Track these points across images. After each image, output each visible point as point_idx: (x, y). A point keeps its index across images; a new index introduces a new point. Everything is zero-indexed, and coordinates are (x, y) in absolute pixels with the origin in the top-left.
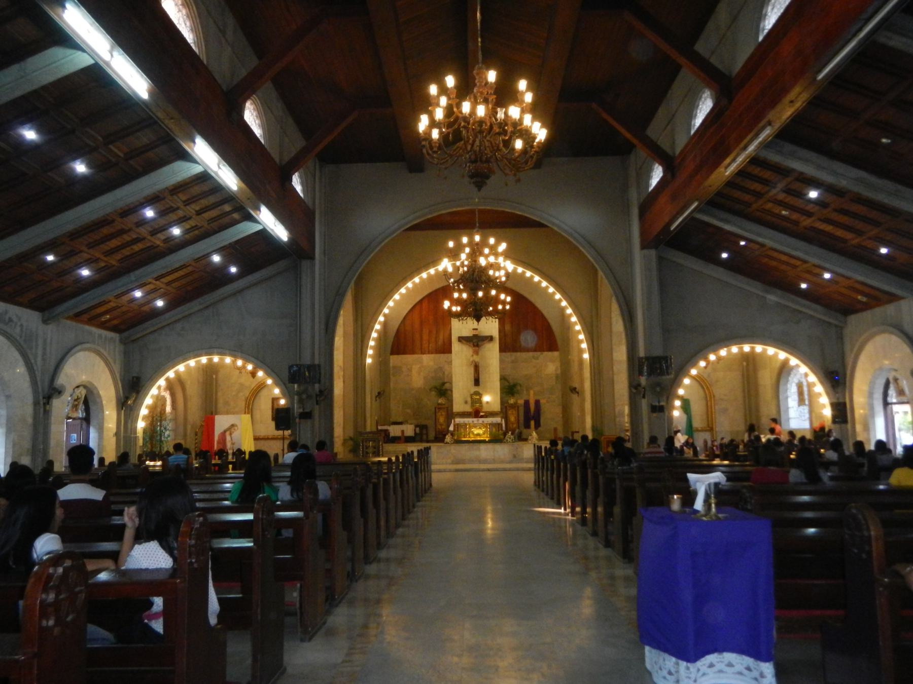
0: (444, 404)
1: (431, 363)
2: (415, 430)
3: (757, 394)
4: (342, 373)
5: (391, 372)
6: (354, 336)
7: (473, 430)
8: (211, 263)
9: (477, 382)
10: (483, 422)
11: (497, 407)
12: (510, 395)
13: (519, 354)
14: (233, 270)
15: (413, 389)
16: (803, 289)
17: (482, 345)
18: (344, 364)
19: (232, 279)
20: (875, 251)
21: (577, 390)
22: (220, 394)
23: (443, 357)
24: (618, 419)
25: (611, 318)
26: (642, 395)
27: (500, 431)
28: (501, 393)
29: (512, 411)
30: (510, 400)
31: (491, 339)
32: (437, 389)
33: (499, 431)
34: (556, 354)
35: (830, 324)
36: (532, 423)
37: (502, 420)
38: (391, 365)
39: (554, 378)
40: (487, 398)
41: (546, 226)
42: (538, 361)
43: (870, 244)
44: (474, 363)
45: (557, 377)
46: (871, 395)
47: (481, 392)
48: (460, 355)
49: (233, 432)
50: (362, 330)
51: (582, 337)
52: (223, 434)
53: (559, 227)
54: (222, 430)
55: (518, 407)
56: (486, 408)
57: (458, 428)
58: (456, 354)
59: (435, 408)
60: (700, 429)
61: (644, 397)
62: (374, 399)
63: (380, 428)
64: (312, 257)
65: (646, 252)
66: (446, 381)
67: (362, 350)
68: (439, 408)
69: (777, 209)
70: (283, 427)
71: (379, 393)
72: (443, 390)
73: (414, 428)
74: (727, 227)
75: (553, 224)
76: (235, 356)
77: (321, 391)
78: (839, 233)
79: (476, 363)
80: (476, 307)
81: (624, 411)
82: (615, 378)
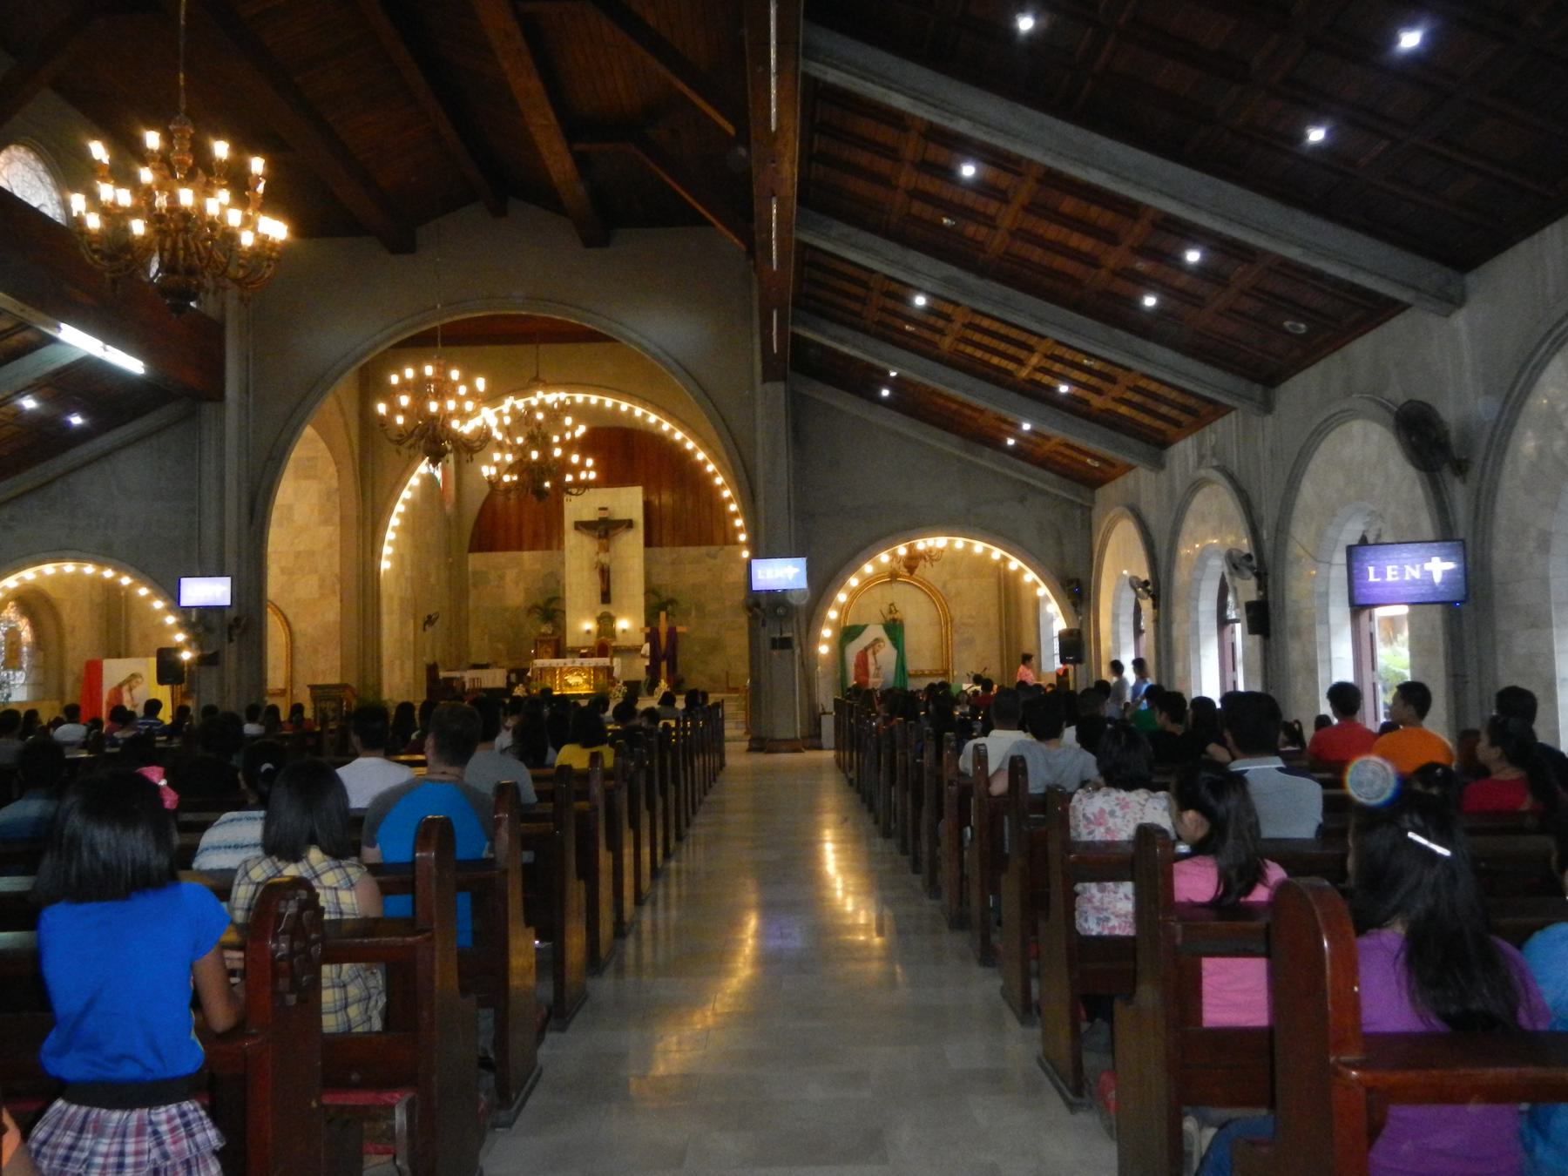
1: (538, 566)
2: (508, 678)
3: (1019, 616)
5: (470, 581)
7: (566, 678)
8: (20, 413)
9: (606, 597)
10: (582, 664)
11: (639, 639)
13: (683, 549)
14: (76, 420)
16: (1012, 446)
17: (614, 535)
18: (341, 568)
19: (82, 435)
20: (1054, 390)
22: (134, 622)
31: (629, 524)
32: (541, 609)
35: (1073, 502)
36: (664, 665)
37: (611, 662)
38: (470, 569)
40: (623, 624)
41: (617, 341)
43: (1046, 379)
44: (599, 566)
46: (1115, 617)
47: (613, 612)
48: (578, 552)
49: (135, 687)
52: (118, 691)
53: (639, 345)
54: (115, 685)
56: (620, 641)
58: (571, 551)
59: (536, 640)
60: (926, 672)
61: (764, 625)
62: (420, 631)
63: (442, 674)
64: (218, 395)
65: (768, 385)
68: (540, 642)
69: (898, 322)
71: (429, 617)
72: (551, 610)
73: (506, 674)
74: (845, 349)
75: (630, 340)
76: (102, 564)
77: (237, 620)
78: (995, 360)
79: (603, 566)
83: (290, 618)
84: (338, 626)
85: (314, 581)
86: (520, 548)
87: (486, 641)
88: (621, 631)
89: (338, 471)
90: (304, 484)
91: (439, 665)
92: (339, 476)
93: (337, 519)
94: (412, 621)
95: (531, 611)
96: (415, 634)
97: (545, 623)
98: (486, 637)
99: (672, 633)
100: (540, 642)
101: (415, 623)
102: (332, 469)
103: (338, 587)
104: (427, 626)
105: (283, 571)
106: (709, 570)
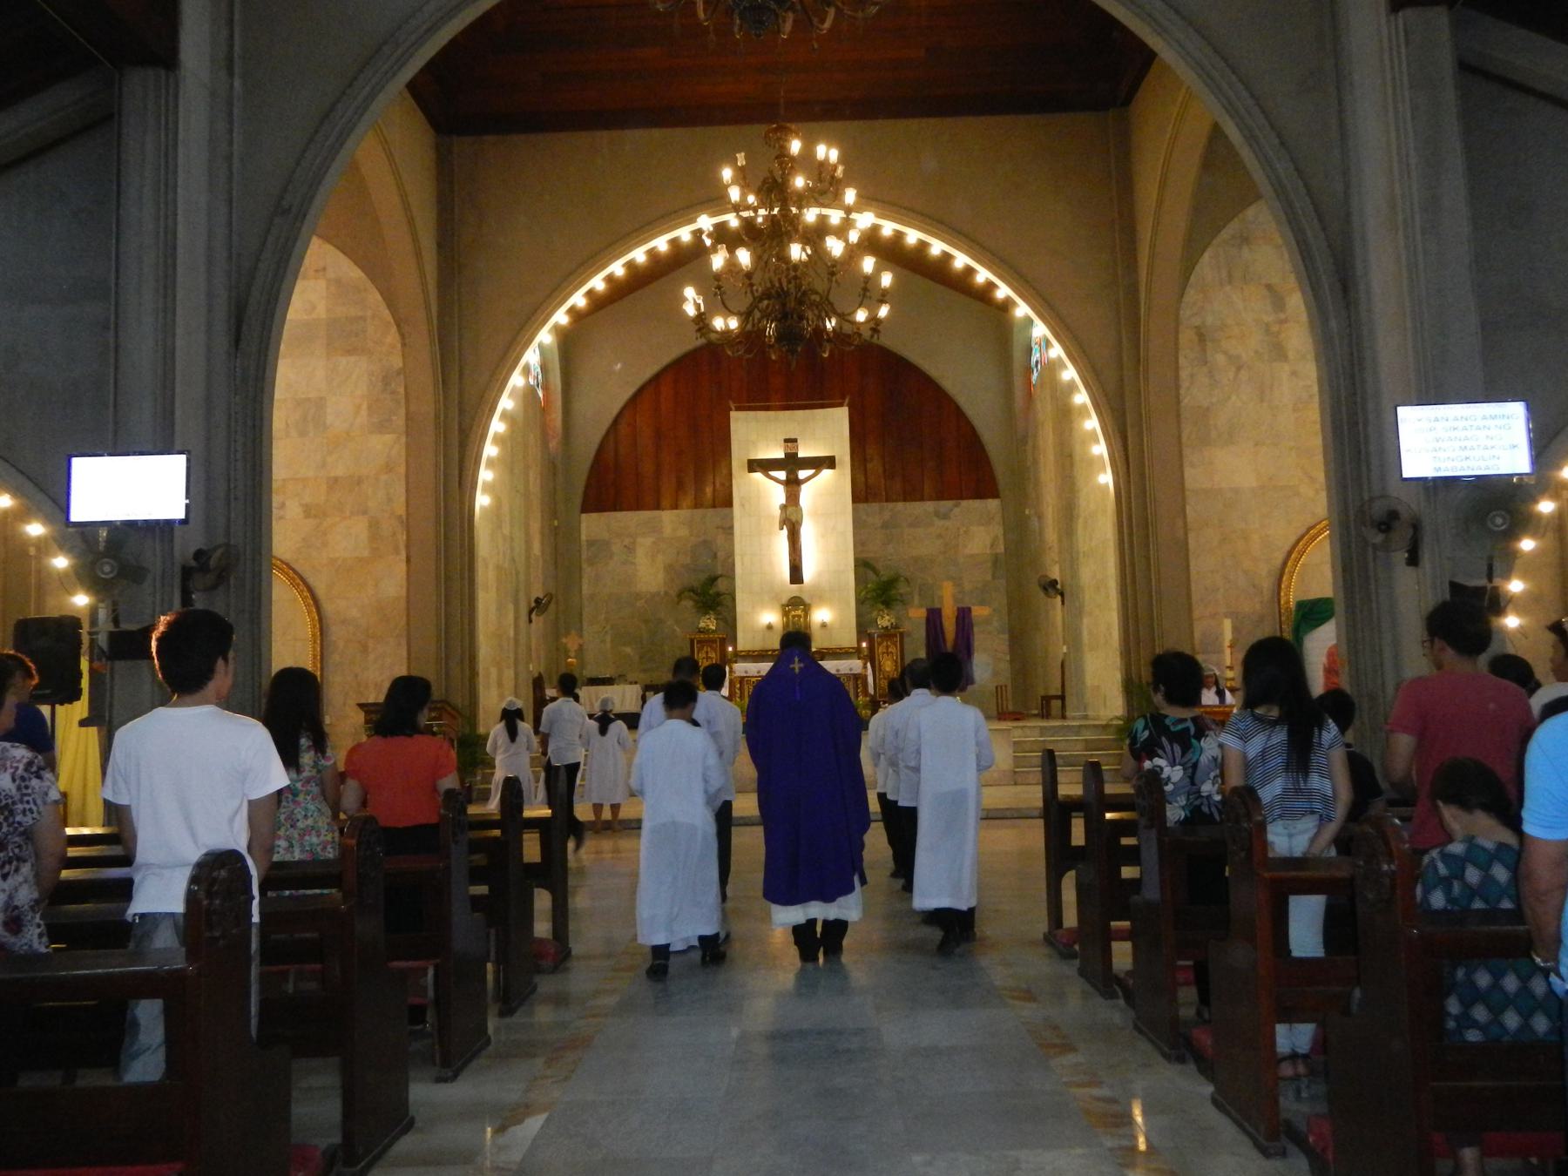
0: (713, 631)
1: (683, 532)
4: (405, 537)
5: (584, 557)
6: (437, 425)
11: (848, 638)
12: (881, 607)
13: (900, 505)
15: (638, 596)
21: (1059, 586)
23: (712, 516)
25: (1177, 369)
26: (1401, 556)
27: (861, 698)
28: (860, 602)
29: (887, 647)
30: (883, 617)
33: (857, 696)
34: (993, 504)
37: (865, 667)
38: (583, 537)
39: (989, 564)
40: (821, 615)
42: (948, 523)
45: (996, 561)
50: (461, 411)
55: (902, 635)
57: (741, 689)
59: (692, 641)
61: (1413, 560)
64: (167, 59)
66: (720, 573)
68: (699, 642)
70: (48, 691)
71: (538, 601)
73: (641, 693)
77: (199, 554)
80: (784, 305)
81: (1218, 637)
82: (1192, 542)
83: (321, 591)
84: (403, 604)
85: (360, 527)
87: (608, 645)
88: (819, 625)
89: (402, 336)
90: (344, 362)
91: (544, 675)
92: (404, 345)
93: (399, 420)
94: (511, 607)
96: (517, 633)
98: (608, 638)
99: (964, 616)
100: (699, 642)
101: (517, 611)
102: (392, 337)
103: (402, 538)
104: (534, 613)
105: (308, 511)
106: (940, 536)
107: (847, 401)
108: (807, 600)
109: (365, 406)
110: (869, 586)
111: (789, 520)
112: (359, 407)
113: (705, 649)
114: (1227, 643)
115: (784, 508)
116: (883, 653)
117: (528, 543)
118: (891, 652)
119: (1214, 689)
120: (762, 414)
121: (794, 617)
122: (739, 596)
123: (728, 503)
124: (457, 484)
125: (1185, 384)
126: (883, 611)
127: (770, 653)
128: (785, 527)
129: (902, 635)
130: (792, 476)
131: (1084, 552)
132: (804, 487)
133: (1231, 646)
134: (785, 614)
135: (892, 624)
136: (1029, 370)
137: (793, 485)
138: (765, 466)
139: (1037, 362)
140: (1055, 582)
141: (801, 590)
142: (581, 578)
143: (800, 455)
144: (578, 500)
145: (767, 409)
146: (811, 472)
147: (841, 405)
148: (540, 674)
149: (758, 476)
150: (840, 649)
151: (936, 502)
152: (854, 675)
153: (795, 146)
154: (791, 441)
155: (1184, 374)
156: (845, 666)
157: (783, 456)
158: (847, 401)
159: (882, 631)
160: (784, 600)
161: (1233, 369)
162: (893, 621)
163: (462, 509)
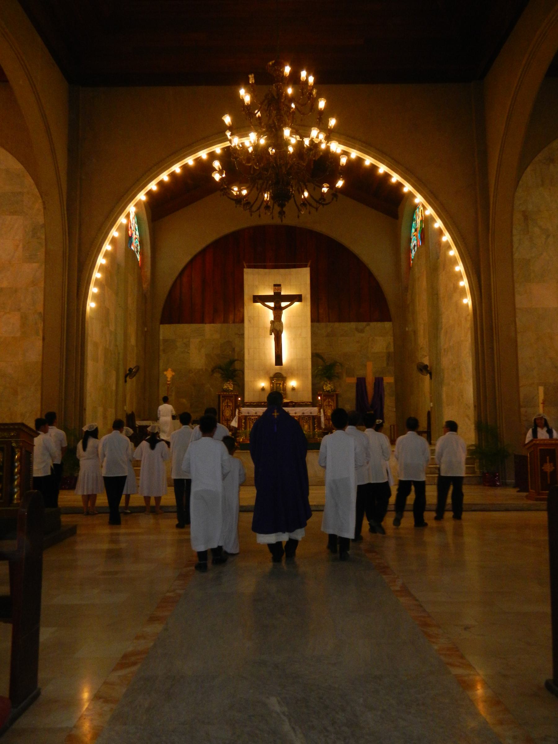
0: (231, 391)
1: (217, 336)
11: (307, 397)
12: (326, 379)
13: (337, 325)
21: (429, 369)
24: (523, 410)
25: (512, 235)
28: (314, 376)
29: (329, 402)
30: (327, 385)
33: (314, 429)
34: (388, 325)
37: (320, 412)
38: (161, 338)
40: (292, 383)
45: (389, 355)
51: (460, 268)
57: (245, 423)
58: (250, 321)
59: (219, 396)
66: (236, 358)
67: (78, 287)
68: (224, 397)
71: (130, 370)
82: (519, 339)
86: (202, 321)
89: (44, 202)
92: (45, 208)
93: (41, 254)
94: (114, 373)
95: (216, 369)
97: (227, 381)
99: (379, 382)
100: (223, 397)
102: (39, 205)
103: (40, 325)
104: (128, 379)
106: (358, 342)
107: (309, 264)
108: (284, 375)
109: (21, 246)
110: (319, 367)
111: (276, 330)
112: (18, 246)
113: (226, 401)
114: (541, 401)
115: (272, 322)
116: (327, 405)
117: (126, 334)
118: (331, 405)
119: (545, 429)
120: (262, 271)
121: (277, 384)
122: (246, 371)
123: (242, 321)
124: (76, 295)
125: (516, 245)
126: (326, 381)
127: (263, 404)
128: (273, 333)
129: (337, 395)
130: (277, 305)
131: (444, 349)
132: (284, 312)
133: (543, 403)
134: (271, 383)
135: (332, 389)
136: (410, 251)
137: (278, 310)
138: (263, 299)
139: (414, 246)
140: (426, 367)
141: (281, 369)
142: (159, 360)
143: (283, 293)
144: (159, 316)
145: (265, 267)
146: (288, 303)
147: (305, 266)
148: (133, 412)
149: (259, 305)
150: (303, 402)
151: (357, 323)
152: (313, 416)
153: (287, 70)
154: (277, 286)
155: (515, 239)
156: (307, 411)
157: (272, 293)
158: (309, 264)
159: (326, 393)
160: (272, 375)
161: (545, 237)
162: (332, 387)
163: (78, 310)
